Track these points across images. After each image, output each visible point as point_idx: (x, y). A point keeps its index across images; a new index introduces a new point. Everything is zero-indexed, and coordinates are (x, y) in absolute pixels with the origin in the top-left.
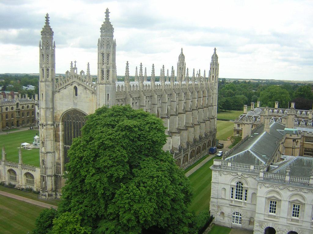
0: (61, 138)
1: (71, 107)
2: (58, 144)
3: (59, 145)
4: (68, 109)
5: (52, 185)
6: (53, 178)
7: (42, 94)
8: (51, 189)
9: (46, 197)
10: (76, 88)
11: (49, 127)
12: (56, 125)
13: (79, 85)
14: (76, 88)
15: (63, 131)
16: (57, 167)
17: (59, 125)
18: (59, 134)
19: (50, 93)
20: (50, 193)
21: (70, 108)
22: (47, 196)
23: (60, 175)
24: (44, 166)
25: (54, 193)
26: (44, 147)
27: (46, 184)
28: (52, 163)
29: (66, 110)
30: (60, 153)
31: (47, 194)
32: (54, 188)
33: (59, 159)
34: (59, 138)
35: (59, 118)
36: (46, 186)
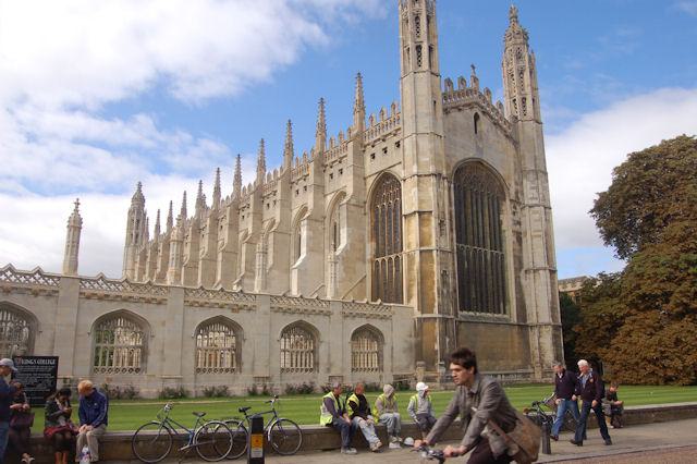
4: (467, 157)
10: (476, 117)
14: (476, 117)
21: (471, 155)
24: (445, 291)
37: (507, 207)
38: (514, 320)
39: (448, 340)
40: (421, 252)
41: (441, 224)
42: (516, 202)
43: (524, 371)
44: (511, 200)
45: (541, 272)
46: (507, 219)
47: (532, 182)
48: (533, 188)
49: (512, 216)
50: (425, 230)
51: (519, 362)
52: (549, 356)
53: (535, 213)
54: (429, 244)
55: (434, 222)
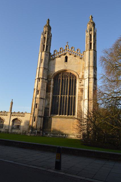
0: (52, 89)
2: (49, 93)
5: (41, 124)
6: (43, 119)
7: (42, 59)
8: (39, 128)
9: (35, 134)
10: (66, 58)
13: (70, 54)
14: (66, 58)
15: (54, 85)
17: (51, 80)
19: (47, 59)
21: (62, 69)
22: (36, 133)
30: (49, 100)
32: (42, 127)
34: (50, 89)
35: (52, 76)
37: (78, 81)
38: (76, 117)
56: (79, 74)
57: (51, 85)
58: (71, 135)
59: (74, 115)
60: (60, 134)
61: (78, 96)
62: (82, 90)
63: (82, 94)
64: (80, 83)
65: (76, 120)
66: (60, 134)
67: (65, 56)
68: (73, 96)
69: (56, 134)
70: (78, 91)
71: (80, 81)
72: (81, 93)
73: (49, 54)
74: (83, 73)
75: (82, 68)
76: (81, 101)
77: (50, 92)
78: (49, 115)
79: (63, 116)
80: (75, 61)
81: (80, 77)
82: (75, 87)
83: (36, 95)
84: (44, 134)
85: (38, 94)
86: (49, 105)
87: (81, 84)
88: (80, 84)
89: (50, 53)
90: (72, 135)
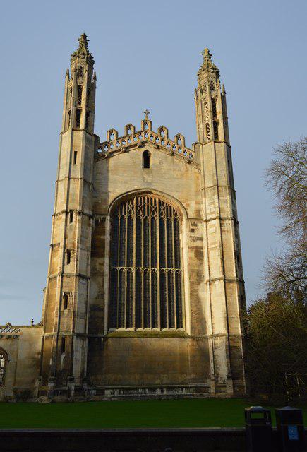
1: (136, 185)
2: (99, 260)
3: (103, 265)
4: (128, 190)
5: (83, 360)
6: (86, 344)
7: (76, 153)
9: (69, 396)
10: (146, 156)
11: (87, 218)
12: (96, 222)
14: (146, 156)
15: (111, 234)
16: (91, 317)
17: (104, 220)
18: (103, 242)
19: (91, 155)
20: (78, 384)
21: (136, 187)
22: (73, 392)
23: (100, 335)
25: (85, 386)
26: (69, 266)
27: (72, 358)
28: (86, 303)
29: (123, 192)
30: (103, 279)
31: (73, 388)
32: (85, 370)
33: (101, 295)
36: (72, 365)
38: (189, 332)
39: (63, 356)
40: (50, 279)
41: (68, 253)
42: (197, 220)
43: (199, 385)
44: (188, 219)
45: (217, 282)
46: (184, 237)
47: (211, 198)
48: (210, 204)
49: (189, 234)
50: (55, 259)
51: (193, 376)
52: (224, 370)
53: (212, 226)
54: (56, 271)
55: (60, 252)
56: (188, 205)
57: (103, 233)
58: (178, 388)
59: (180, 325)
60: (144, 388)
61: (191, 271)
62: (199, 253)
63: (201, 264)
64: (193, 231)
65: (190, 340)
66: (144, 388)
67: (143, 150)
68: (174, 270)
69: (134, 389)
70: (186, 255)
71: (192, 227)
72: (196, 261)
73: (93, 139)
74: (198, 203)
75: (193, 187)
76: (199, 284)
77: (103, 256)
78: (106, 328)
79: (149, 329)
80: (172, 168)
81: (192, 213)
82: (177, 242)
83: (63, 265)
84: (94, 392)
85: (69, 262)
86: (103, 298)
87: (196, 234)
88: (192, 234)
89: (97, 138)
90: (182, 388)
